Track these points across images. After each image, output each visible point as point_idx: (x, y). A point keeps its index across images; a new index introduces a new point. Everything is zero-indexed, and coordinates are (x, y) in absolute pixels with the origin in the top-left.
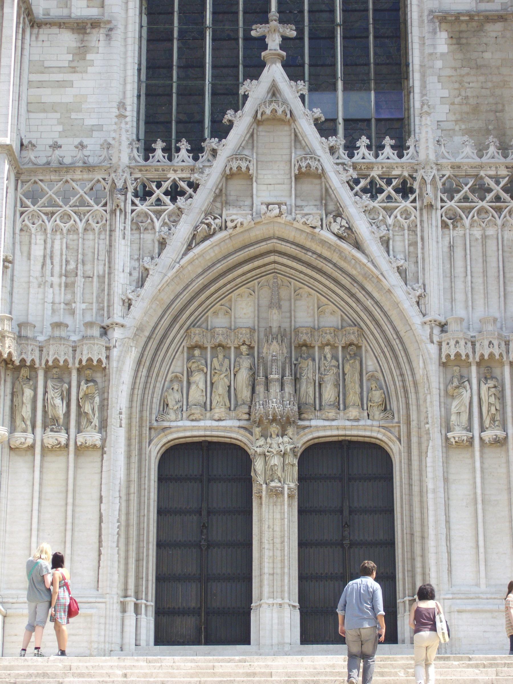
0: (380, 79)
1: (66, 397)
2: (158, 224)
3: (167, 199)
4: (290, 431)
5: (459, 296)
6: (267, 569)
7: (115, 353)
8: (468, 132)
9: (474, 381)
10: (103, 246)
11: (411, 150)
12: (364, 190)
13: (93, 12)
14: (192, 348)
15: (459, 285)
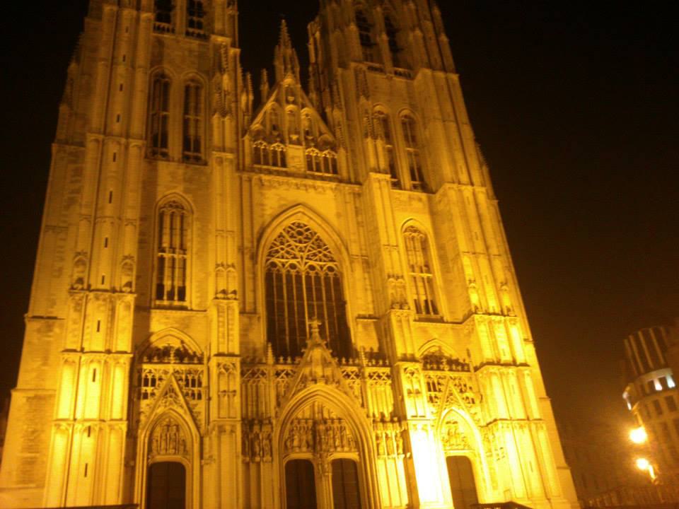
3: (285, 376)
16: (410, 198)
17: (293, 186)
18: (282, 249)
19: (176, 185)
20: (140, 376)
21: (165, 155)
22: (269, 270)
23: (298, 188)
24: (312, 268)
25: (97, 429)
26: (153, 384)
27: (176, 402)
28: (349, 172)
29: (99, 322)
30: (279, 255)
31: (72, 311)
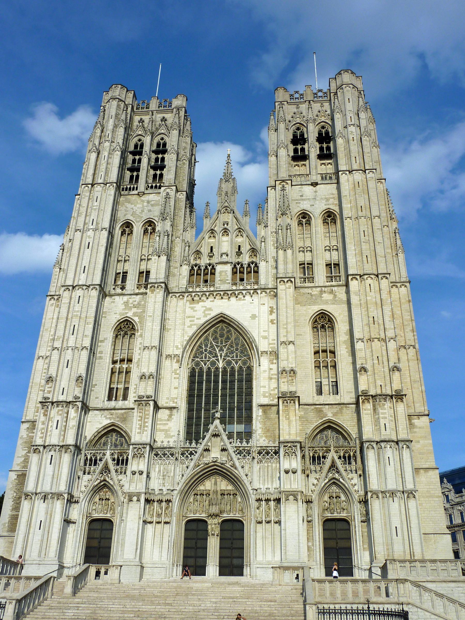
0: (246, 421)
1: (161, 508)
2: (186, 463)
3: (189, 456)
4: (217, 517)
5: (261, 482)
6: (211, 555)
7: (174, 497)
8: (266, 437)
9: (264, 505)
10: (173, 468)
11: (250, 442)
12: (238, 453)
13: (174, 405)
14: (194, 495)
15: (261, 479)
16: (321, 292)
17: (217, 297)
18: (206, 350)
19: (127, 311)
20: (87, 458)
21: (123, 288)
22: (193, 369)
23: (222, 298)
24: (229, 363)
25: (49, 497)
26: (95, 464)
27: (108, 477)
28: (267, 279)
29: (58, 421)
30: (204, 355)
31: (42, 415)
